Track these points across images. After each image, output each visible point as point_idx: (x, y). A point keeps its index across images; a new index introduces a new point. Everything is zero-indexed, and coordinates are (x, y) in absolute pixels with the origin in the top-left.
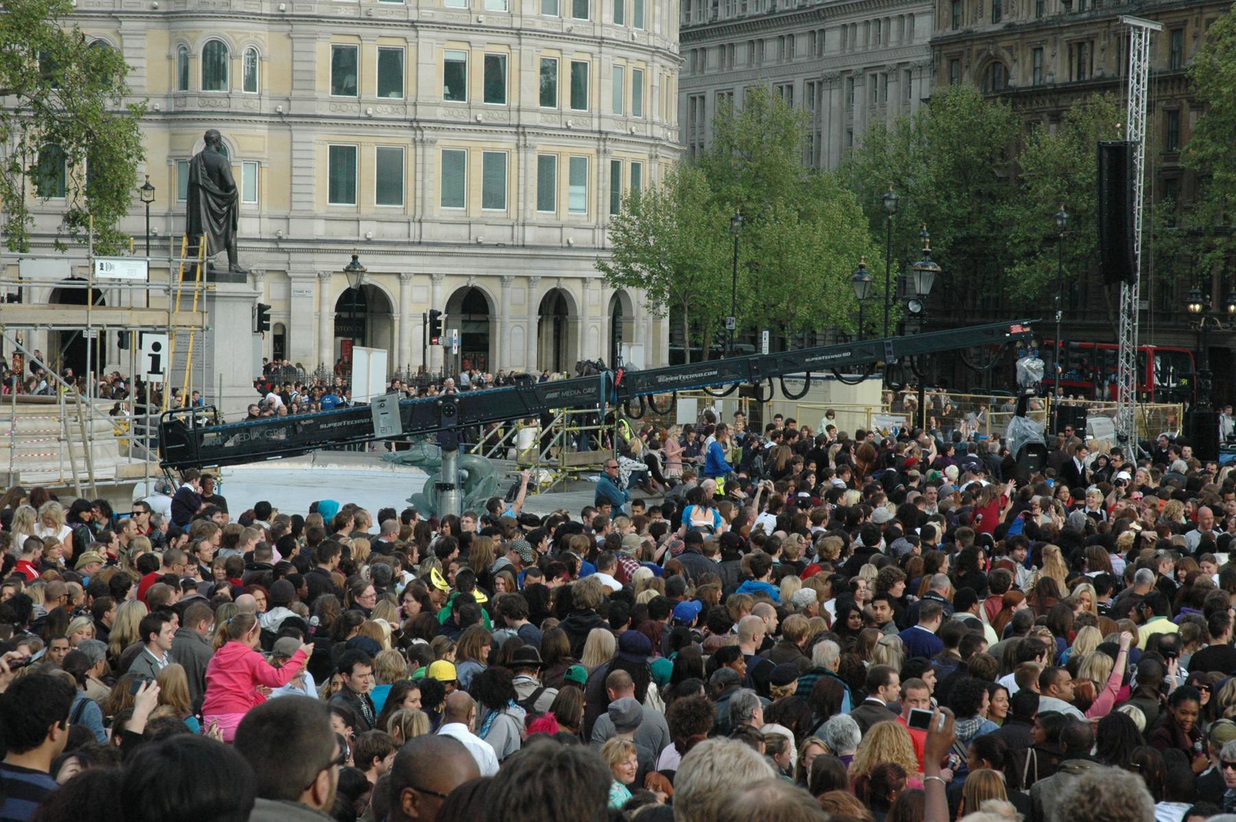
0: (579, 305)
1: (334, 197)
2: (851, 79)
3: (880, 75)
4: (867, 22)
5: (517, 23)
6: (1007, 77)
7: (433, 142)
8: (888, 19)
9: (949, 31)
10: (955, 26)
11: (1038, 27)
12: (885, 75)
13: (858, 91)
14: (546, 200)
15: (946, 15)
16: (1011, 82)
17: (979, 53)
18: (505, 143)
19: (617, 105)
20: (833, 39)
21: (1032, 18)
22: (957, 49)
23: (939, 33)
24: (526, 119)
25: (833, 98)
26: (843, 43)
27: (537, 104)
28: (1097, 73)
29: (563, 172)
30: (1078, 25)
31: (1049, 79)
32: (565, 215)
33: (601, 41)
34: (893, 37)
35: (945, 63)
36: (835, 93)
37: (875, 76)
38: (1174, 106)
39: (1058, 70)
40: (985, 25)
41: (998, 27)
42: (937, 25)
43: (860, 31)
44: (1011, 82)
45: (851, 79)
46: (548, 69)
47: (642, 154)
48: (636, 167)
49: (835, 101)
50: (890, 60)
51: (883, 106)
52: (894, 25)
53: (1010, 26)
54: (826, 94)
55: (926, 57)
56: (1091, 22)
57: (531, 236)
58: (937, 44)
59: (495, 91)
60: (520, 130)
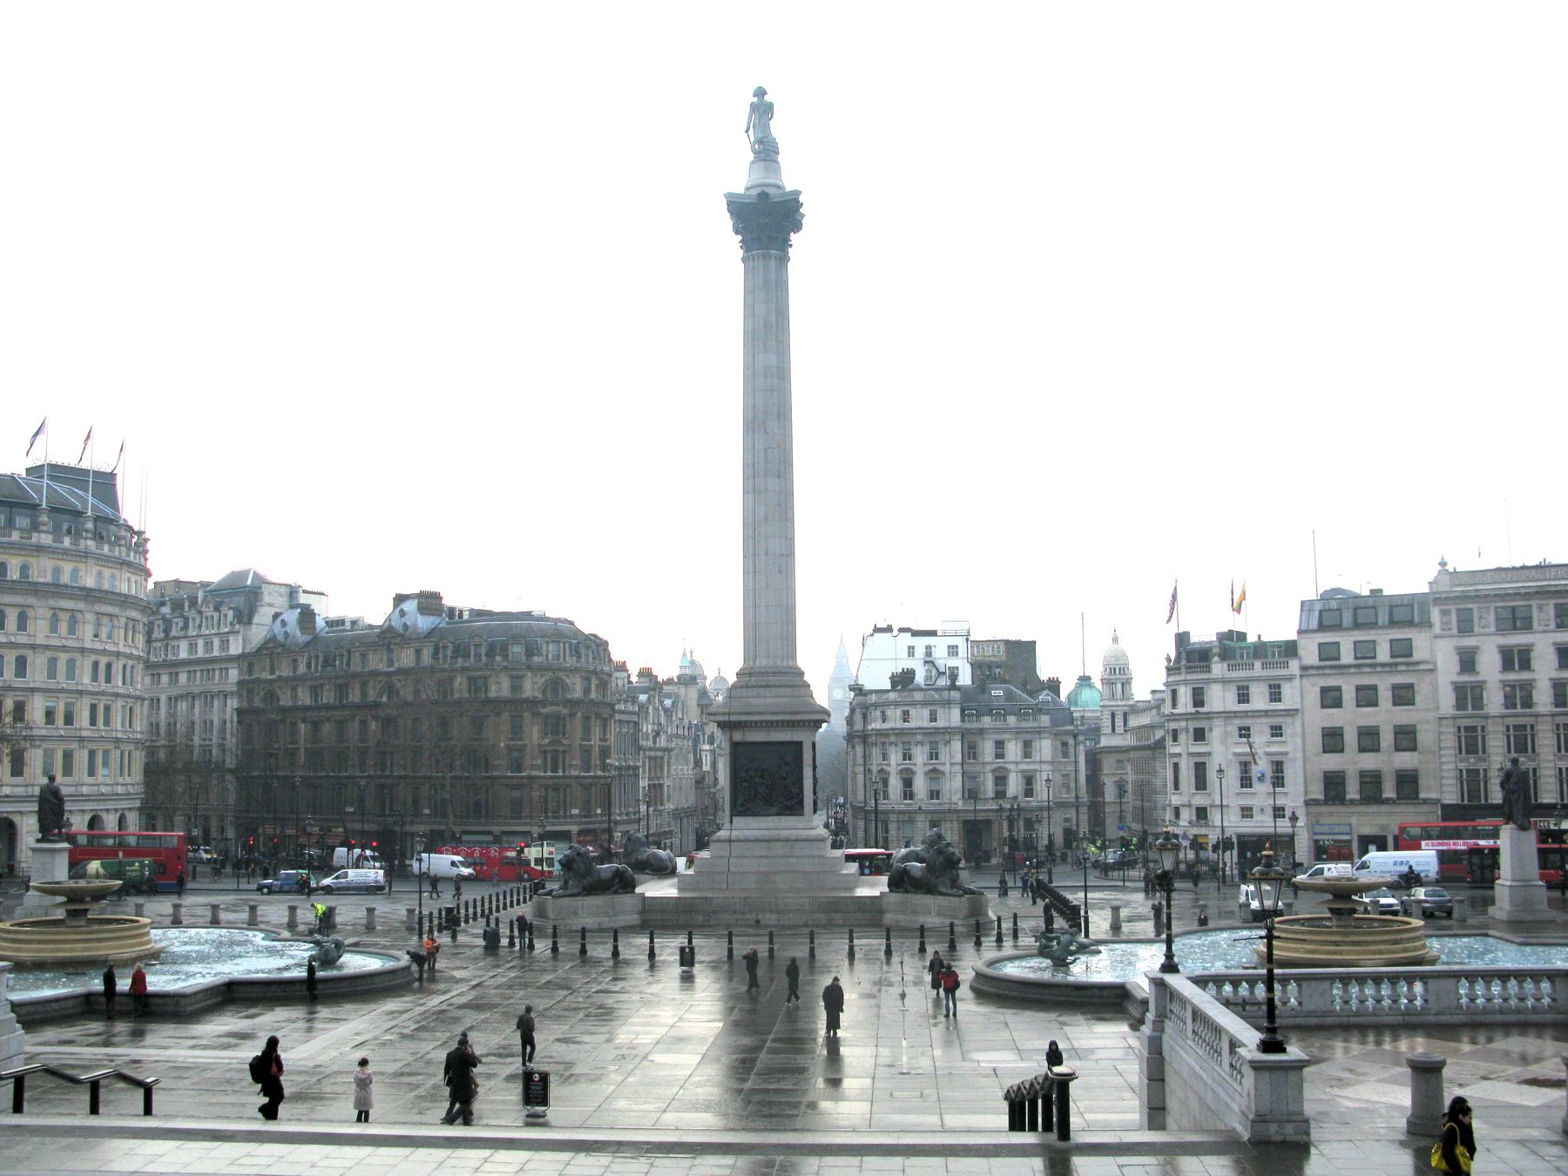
0: (105, 822)
1: (13, 775)
2: (193, 697)
3: (208, 697)
4: (202, 671)
5: (80, 688)
6: (279, 700)
7: (40, 746)
8: (214, 670)
9: (247, 677)
10: (250, 675)
11: (294, 679)
12: (212, 696)
13: (197, 703)
14: (92, 772)
15: (245, 669)
16: (281, 703)
17: (263, 689)
18: (74, 746)
19: (123, 725)
20: (183, 677)
21: (291, 674)
22: (251, 686)
23: (242, 678)
24: (84, 734)
25: (183, 706)
26: (189, 679)
27: (89, 727)
28: (325, 701)
29: (99, 759)
30: (313, 679)
31: (300, 703)
32: (100, 779)
33: (117, 695)
34: (217, 678)
35: (245, 693)
36: (184, 703)
37: (206, 696)
38: (363, 718)
39: (304, 698)
40: (266, 675)
41: (272, 677)
42: (240, 674)
43: (198, 674)
44: (281, 703)
45: (193, 697)
46: (94, 708)
47: (132, 747)
48: (129, 752)
49: (184, 708)
50: (215, 689)
51: (211, 711)
52: (217, 672)
53: (280, 677)
54: (179, 704)
55: (235, 689)
56: (321, 677)
57: (85, 790)
58: (240, 683)
59: (69, 719)
60: (81, 739)
